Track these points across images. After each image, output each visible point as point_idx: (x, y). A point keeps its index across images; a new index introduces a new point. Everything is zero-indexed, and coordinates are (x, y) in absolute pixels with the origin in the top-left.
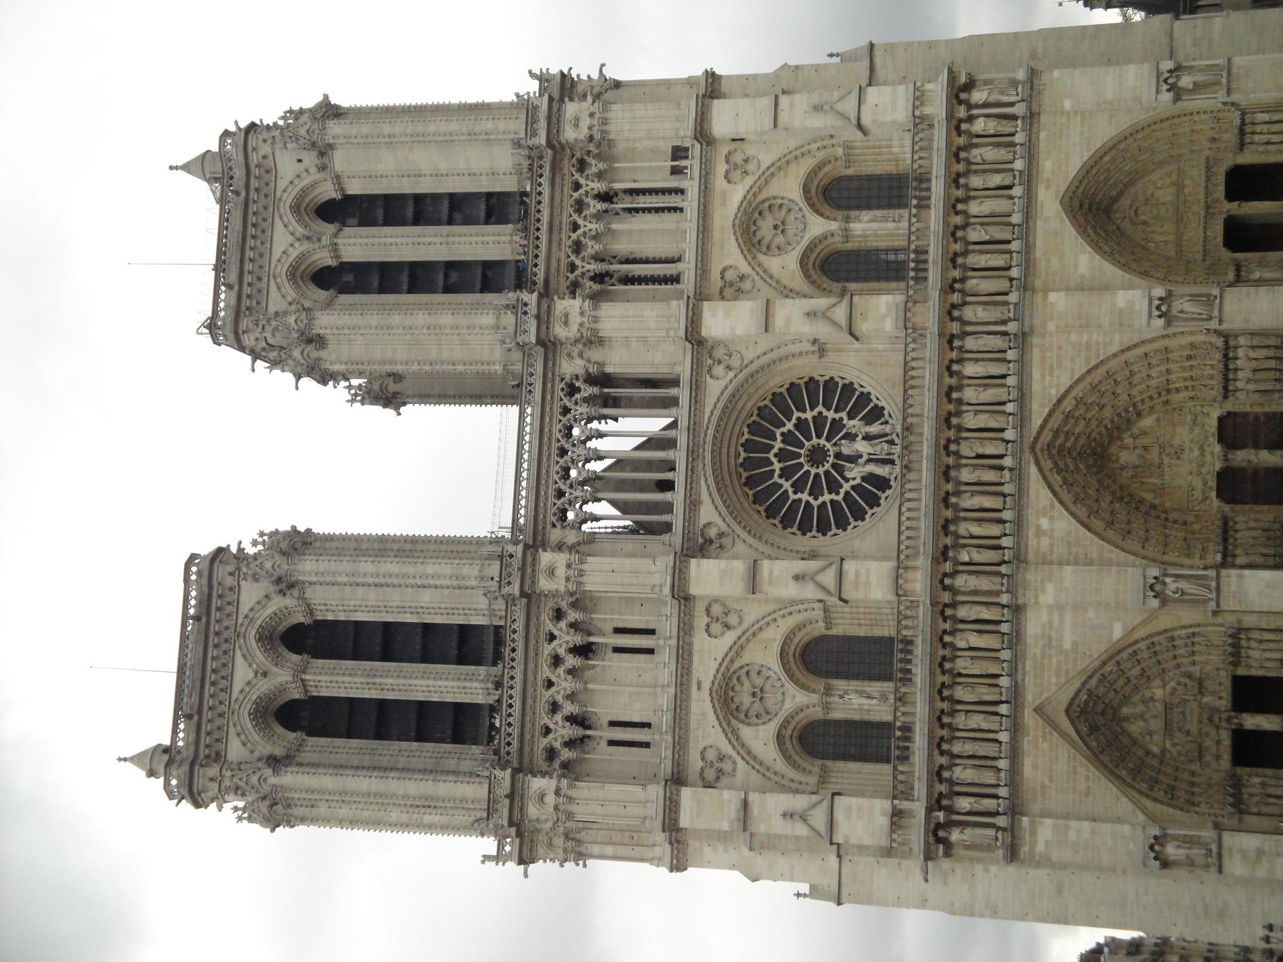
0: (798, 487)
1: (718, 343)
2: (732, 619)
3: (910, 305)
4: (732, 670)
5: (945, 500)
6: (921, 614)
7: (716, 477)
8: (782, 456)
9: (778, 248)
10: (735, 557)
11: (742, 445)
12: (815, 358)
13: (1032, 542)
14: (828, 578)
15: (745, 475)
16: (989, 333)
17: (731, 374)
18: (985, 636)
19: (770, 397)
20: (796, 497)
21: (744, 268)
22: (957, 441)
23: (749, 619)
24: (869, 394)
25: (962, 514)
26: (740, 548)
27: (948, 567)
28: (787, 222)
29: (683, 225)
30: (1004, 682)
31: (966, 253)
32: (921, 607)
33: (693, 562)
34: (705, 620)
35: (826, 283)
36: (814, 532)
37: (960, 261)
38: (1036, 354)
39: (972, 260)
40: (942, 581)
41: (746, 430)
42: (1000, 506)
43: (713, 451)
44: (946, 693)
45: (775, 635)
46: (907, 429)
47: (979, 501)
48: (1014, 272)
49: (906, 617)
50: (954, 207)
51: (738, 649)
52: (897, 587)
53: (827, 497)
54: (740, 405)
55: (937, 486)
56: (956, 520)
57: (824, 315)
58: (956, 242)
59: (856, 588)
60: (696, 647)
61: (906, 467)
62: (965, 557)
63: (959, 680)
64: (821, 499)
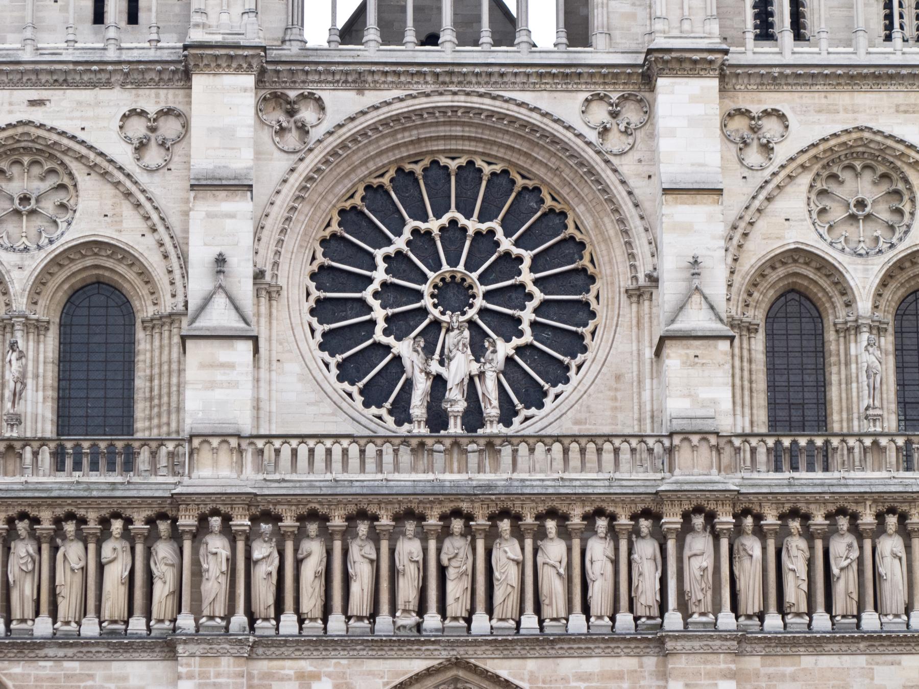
0: (396, 262)
1: (648, 109)
2: (154, 156)
3: (713, 440)
4: (66, 160)
5: (362, 515)
6: (160, 479)
7: (407, 116)
8: (453, 231)
9: (823, 211)
11: (471, 163)
12: (625, 282)
13: (289, 667)
14: (220, 316)
15: (418, 169)
16: (663, 581)
17: (592, 136)
18: (123, 591)
19: (558, 207)
20: (379, 260)
21: (782, 153)
22: (468, 532)
23: (154, 184)
24: (567, 380)
25: (337, 545)
26: (280, 164)
27: (241, 522)
28: (870, 225)
29: (862, 41)
30: (43, 626)
31: (809, 535)
32: (171, 479)
33: (249, 80)
34: (152, 109)
35: (765, 297)
36: (316, 294)
37: (795, 525)
38: (627, 663)
39: (797, 546)
40: (215, 512)
41: (498, 168)
42: (354, 609)
43: (454, 110)
44: (22, 526)
45: (129, 232)
47: (362, 573)
48: (773, 621)
49: (154, 454)
50: (892, 511)
51: (103, 168)
52: (205, 437)
53: (379, 314)
54: (540, 155)
55: (384, 499)
56: (326, 535)
58: (828, 516)
60: (102, 94)
61: (422, 445)
62: (260, 550)
63: (45, 547)
64: (376, 304)
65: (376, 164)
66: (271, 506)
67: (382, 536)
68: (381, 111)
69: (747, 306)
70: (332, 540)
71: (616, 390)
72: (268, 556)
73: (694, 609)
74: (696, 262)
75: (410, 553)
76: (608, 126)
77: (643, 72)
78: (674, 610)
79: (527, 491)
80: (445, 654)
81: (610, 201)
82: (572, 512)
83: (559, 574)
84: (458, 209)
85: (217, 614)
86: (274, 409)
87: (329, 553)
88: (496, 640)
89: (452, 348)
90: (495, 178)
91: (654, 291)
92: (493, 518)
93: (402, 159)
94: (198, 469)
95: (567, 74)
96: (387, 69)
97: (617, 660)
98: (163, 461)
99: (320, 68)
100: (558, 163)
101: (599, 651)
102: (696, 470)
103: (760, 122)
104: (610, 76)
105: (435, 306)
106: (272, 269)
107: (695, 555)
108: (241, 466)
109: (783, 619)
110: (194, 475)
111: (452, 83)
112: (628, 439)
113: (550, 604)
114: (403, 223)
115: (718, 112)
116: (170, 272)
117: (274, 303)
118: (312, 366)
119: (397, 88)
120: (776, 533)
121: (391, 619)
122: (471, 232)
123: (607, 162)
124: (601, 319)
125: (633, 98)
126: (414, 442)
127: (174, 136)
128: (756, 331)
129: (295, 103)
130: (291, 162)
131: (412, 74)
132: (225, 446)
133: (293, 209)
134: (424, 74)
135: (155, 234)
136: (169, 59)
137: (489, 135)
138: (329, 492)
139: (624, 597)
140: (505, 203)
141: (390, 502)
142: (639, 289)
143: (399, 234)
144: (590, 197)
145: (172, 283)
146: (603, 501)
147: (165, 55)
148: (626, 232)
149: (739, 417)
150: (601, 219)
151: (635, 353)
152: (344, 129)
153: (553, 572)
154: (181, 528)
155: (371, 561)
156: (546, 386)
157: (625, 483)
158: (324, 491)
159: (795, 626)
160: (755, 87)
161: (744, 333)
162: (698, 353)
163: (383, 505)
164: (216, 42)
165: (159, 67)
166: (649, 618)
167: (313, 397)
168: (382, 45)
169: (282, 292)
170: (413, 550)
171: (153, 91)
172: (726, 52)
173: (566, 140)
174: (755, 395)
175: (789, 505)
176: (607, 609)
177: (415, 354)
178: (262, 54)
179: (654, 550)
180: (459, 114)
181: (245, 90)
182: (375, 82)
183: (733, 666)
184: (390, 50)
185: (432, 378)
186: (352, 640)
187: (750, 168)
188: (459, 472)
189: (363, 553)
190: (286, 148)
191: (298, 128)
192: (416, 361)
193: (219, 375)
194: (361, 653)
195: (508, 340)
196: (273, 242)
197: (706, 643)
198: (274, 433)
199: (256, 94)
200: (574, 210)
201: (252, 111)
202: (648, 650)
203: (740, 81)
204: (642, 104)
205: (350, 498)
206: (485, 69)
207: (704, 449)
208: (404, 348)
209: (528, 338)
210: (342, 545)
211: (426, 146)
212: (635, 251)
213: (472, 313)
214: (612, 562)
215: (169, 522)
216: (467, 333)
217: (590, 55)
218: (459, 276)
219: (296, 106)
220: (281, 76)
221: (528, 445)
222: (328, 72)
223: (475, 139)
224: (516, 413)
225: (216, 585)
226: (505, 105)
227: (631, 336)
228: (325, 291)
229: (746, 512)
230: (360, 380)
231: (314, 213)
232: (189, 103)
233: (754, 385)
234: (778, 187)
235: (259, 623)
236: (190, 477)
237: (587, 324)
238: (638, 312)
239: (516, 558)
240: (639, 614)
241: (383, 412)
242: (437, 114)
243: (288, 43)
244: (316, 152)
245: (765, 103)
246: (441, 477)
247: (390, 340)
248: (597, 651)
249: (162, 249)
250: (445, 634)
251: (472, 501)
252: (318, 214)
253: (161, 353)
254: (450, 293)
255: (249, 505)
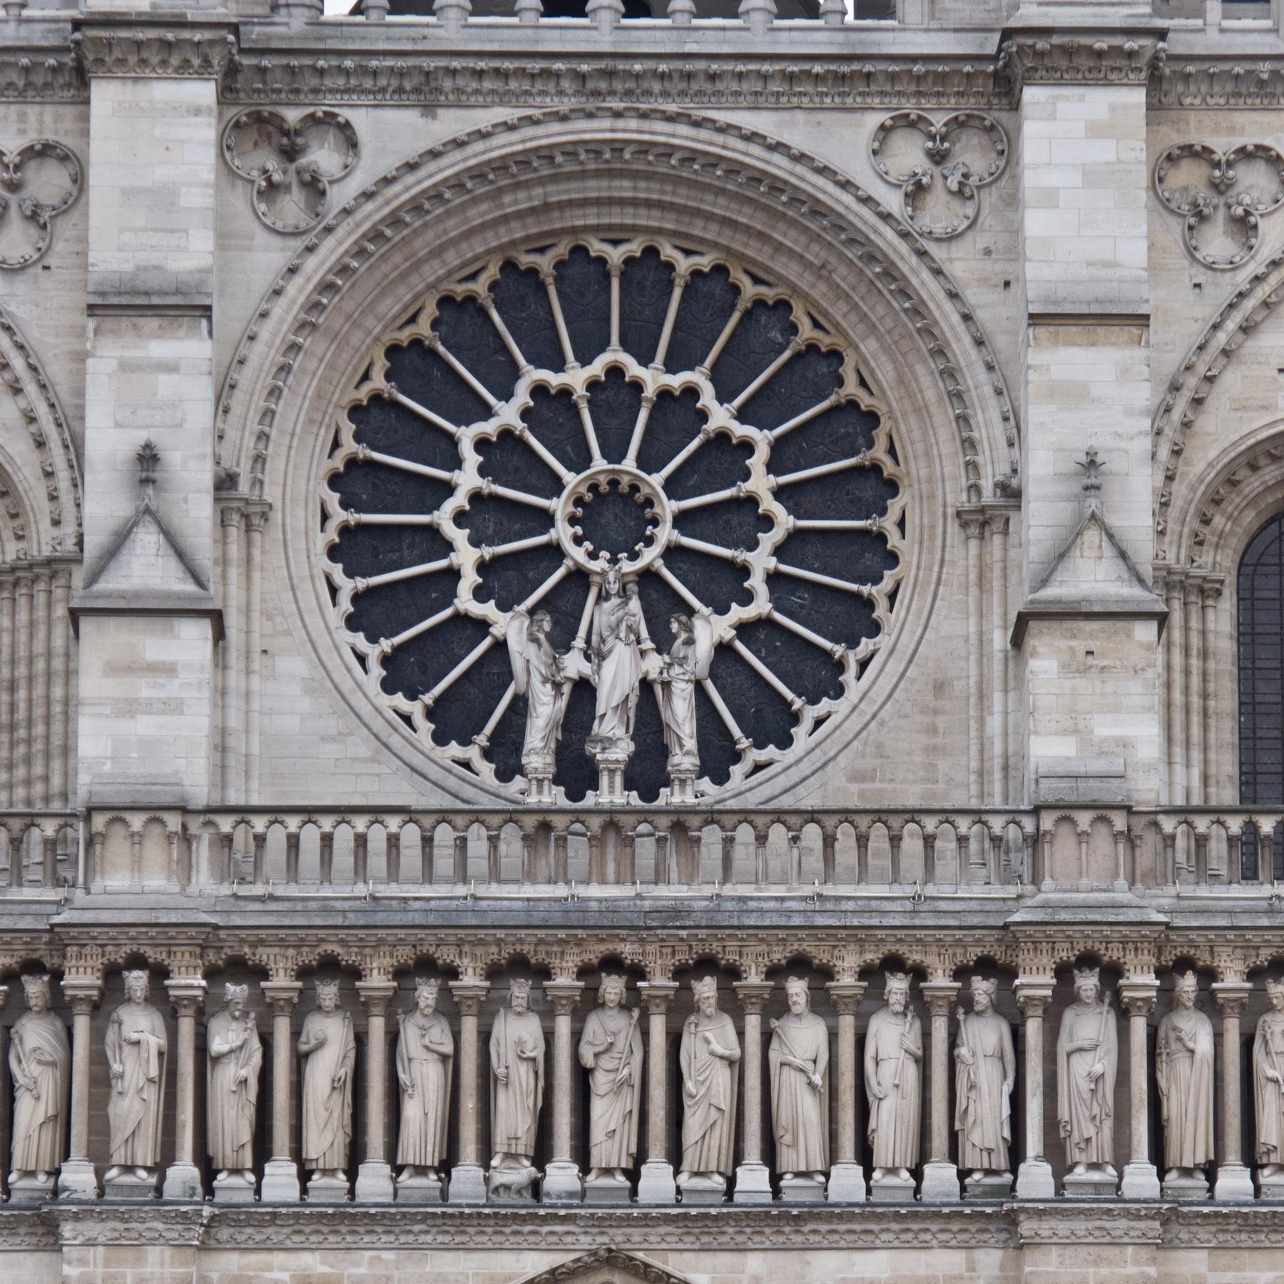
0: (502, 453)
1: (1006, 147)
3: (1120, 821)
6: (28, 893)
7: (523, 160)
8: (615, 393)
10: (225, 238)
11: (651, 252)
12: (957, 497)
14: (146, 569)
15: (545, 263)
17: (893, 201)
19: (825, 342)
22: (634, 1002)
24: (839, 692)
25: (377, 1026)
26: (268, 257)
27: (188, 980)
32: (51, 894)
33: (205, 92)
35: (1234, 525)
36: (340, 516)
38: (945, 1261)
40: (137, 961)
41: (705, 262)
42: (409, 1152)
43: (617, 147)
46: (679, 828)
48: (1234, 1181)
52: (118, 812)
53: (466, 556)
56: (355, 1006)
57: (1089, 521)
59: (112, 669)
64: (459, 536)
65: (461, 258)
66: (247, 950)
67: (464, 1009)
68: (470, 150)
69: (1200, 543)
70: (367, 1015)
71: (936, 712)
72: (241, 1047)
73: (1077, 1156)
74: (1092, 463)
75: (520, 1042)
76: (925, 180)
77: (996, 71)
78: (1037, 1158)
79: (751, 921)
80: (585, 1242)
81: (927, 332)
82: (839, 963)
83: (811, 1084)
84: (626, 345)
85: (139, 1162)
86: (255, 749)
87: (361, 1040)
88: (686, 1216)
89: (605, 634)
90: (700, 283)
91: (1013, 515)
92: (682, 973)
93: (513, 244)
94: (102, 873)
95: (844, 76)
96: (482, 64)
97: (923, 1256)
98: (35, 853)
99: (348, 63)
100: (823, 254)
101: (890, 1236)
102: (1084, 882)
103: (1231, 173)
104: (930, 79)
105: (578, 541)
106: (253, 470)
107: (1080, 1050)
108: (186, 868)
109: (1254, 1178)
110: (96, 886)
111: (612, 93)
112: (952, 817)
113: (794, 1145)
114: (516, 373)
115: (1143, 156)
116: (49, 475)
117: (257, 537)
118: (333, 662)
119: (501, 104)
120: (1243, 1006)
121: (481, 1172)
122: (650, 392)
123: (922, 254)
124: (908, 568)
125: (977, 123)
126: (530, 822)
127: (55, 201)
128: (1219, 593)
129: (298, 133)
130: (289, 254)
131: (533, 76)
132: (156, 830)
133: (294, 348)
134: (557, 75)
135: (19, 399)
136: (45, 43)
137: (688, 197)
138: (362, 922)
139: (937, 1133)
140: (720, 332)
141: (481, 942)
142: (982, 510)
143: (506, 394)
144: (889, 322)
145: (53, 498)
146: (900, 941)
147: (37, 35)
148: (957, 396)
149: (1179, 769)
150: (910, 367)
151: (973, 639)
152: (397, 188)
153: (800, 1080)
154: (69, 992)
155: (444, 1058)
156: (798, 703)
157: (943, 906)
158: (352, 919)
159: (1277, 1190)
160: (1222, 101)
161: (1192, 598)
162: (1092, 645)
163: (466, 948)
164: (139, 14)
165: (25, 61)
166: (989, 1172)
167: (331, 724)
168: (472, 14)
169: (271, 515)
170: (526, 1036)
171: (13, 108)
172: (1162, 34)
173: (840, 209)
174: (1212, 722)
175: (1269, 951)
176: (907, 1156)
177: (532, 647)
178: (231, 38)
179: (1001, 1038)
180: (627, 156)
181: (197, 111)
182: (459, 91)
183: (1152, 1271)
184: (489, 26)
185: (567, 689)
186: (404, 1214)
187: (1210, 267)
188: (617, 882)
189: (426, 1041)
190: (279, 226)
191: (303, 184)
192: (534, 661)
193: (145, 689)
194: (422, 1238)
195: (722, 610)
196: (254, 417)
197: (1098, 1223)
198: (256, 801)
199: (220, 115)
200: (857, 348)
201: (209, 155)
202: (986, 1236)
203: (1193, 89)
204: (995, 136)
205: (401, 933)
206: (678, 65)
207: (1102, 841)
208: (510, 626)
209: (762, 605)
210: (387, 1024)
211: (562, 218)
212: (975, 434)
213: (650, 556)
214: (917, 1061)
215: (46, 978)
216: (635, 605)
217: (890, 36)
218: (625, 480)
219: (300, 141)
220: (269, 77)
221: (755, 828)
222: (364, 71)
223: (660, 205)
224: (737, 757)
225: (137, 1104)
226: (719, 138)
227: (967, 602)
228: (358, 511)
229: (1184, 964)
230: (427, 689)
231: (336, 355)
232: (86, 133)
233: (1212, 703)
234: (1266, 304)
235: (222, 1179)
236: (88, 891)
237: (881, 578)
238: (980, 557)
239: (727, 1053)
240: (969, 1165)
241: (473, 753)
242: (583, 157)
243: (283, 11)
244: (340, 232)
245: (1242, 133)
246: (582, 891)
247: (488, 610)
248: (884, 1237)
249: (33, 428)
250: (587, 1201)
251: (642, 941)
252: (345, 356)
253: (31, 636)
254: (608, 515)
255: (203, 948)
